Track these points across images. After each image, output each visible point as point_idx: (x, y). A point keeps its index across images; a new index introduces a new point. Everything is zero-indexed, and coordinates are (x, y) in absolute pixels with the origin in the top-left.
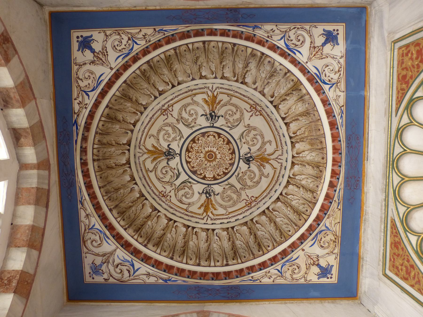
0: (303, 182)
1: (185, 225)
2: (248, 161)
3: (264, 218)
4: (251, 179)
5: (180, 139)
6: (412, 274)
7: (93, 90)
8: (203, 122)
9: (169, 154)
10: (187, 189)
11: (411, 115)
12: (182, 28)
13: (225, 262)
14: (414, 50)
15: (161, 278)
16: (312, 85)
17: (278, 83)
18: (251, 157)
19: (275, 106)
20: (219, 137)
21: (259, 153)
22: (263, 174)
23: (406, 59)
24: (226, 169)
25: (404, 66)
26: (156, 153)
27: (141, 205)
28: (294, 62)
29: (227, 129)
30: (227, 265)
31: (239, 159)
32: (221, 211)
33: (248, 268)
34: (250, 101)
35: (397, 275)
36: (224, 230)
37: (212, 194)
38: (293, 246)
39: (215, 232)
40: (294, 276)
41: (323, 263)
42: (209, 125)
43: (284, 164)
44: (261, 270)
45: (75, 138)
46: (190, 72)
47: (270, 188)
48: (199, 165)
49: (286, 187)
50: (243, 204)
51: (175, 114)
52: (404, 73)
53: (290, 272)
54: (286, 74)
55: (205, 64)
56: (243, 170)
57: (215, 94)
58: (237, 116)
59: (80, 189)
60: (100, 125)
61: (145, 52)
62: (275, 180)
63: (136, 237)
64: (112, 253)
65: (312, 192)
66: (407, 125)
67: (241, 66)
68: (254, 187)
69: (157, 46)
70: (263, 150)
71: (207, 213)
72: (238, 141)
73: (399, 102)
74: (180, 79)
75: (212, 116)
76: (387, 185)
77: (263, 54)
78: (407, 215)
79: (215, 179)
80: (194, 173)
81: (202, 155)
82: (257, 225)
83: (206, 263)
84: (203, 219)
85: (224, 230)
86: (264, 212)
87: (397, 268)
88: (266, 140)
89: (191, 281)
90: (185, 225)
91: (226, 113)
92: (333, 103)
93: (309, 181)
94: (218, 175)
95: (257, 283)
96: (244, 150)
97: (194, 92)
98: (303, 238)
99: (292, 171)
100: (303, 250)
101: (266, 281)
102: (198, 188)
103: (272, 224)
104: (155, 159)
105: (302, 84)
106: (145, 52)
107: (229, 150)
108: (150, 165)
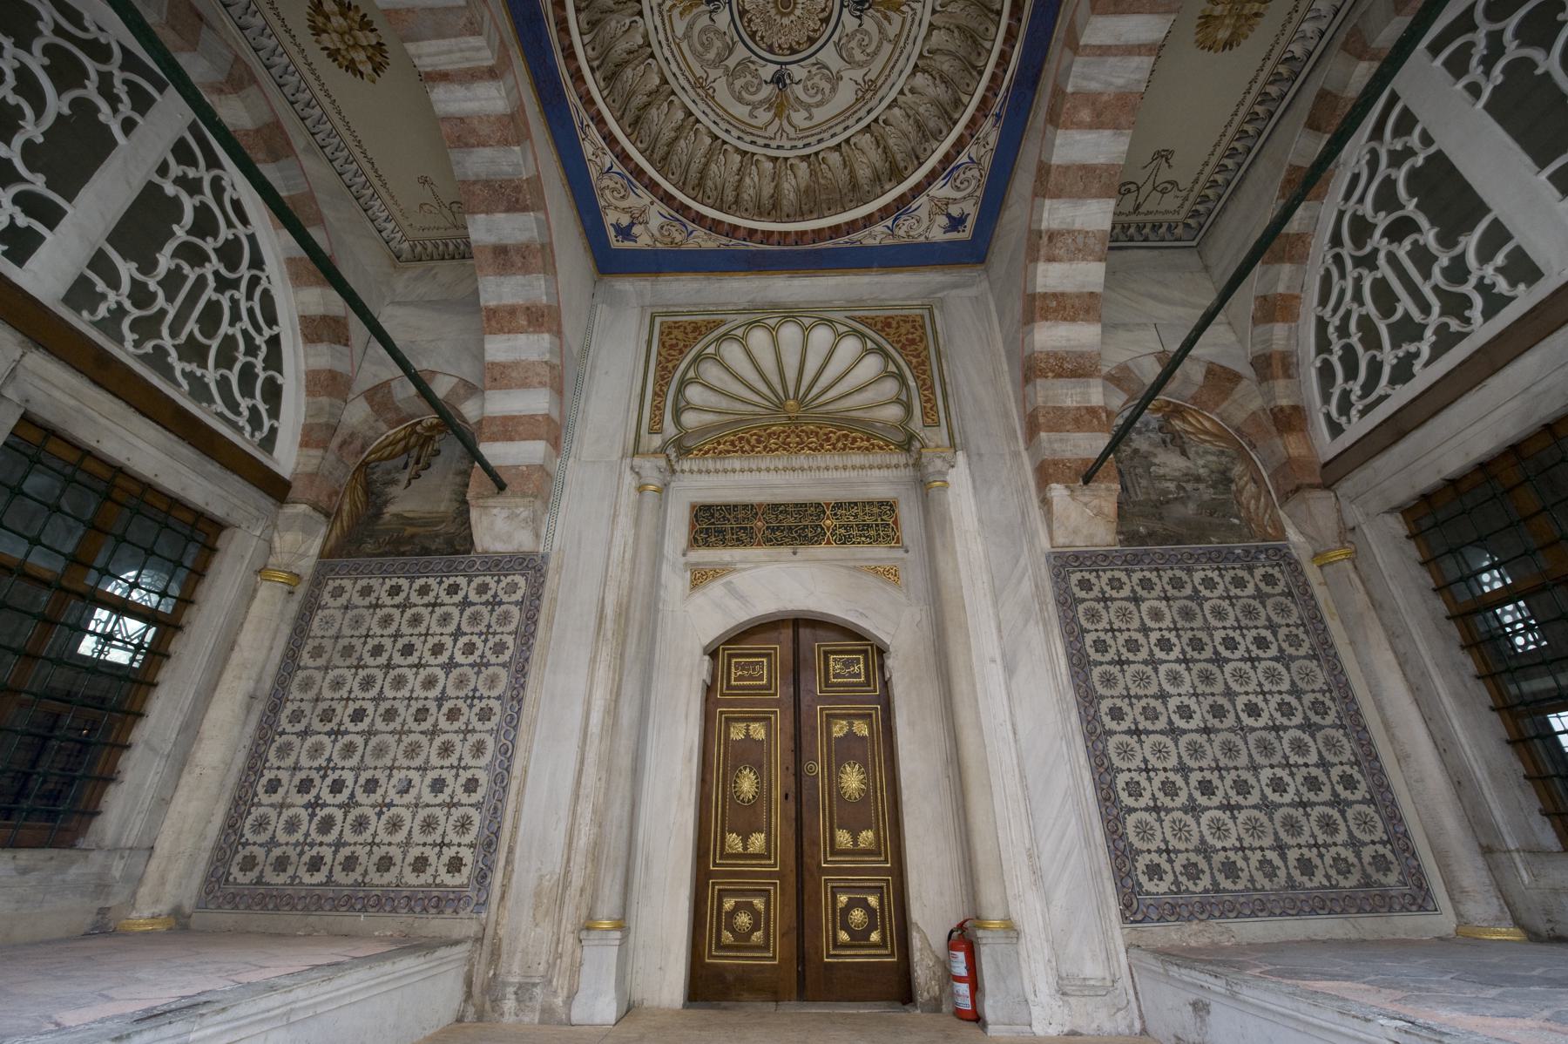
0: (747, 180)
2: (778, 79)
3: (680, 115)
4: (745, 87)
11: (846, 334)
13: (595, 64)
17: (905, 135)
18: (785, 85)
19: (869, 126)
20: (822, 21)
22: (755, 108)
23: (909, 326)
24: (762, 38)
28: (932, 177)
29: (835, 38)
30: (592, 70)
32: (680, 27)
33: (599, 112)
35: (662, 333)
36: (646, 36)
38: (652, 186)
39: (637, 18)
41: (636, 230)
43: (774, 144)
47: (733, 121)
49: (737, 150)
50: (699, 72)
52: (894, 324)
53: (612, 185)
56: (761, 71)
57: (904, 8)
58: (859, 57)
62: (745, 129)
66: (835, 331)
67: (945, 67)
68: (732, 92)
72: (813, 60)
73: (861, 320)
77: (955, 123)
78: (735, 339)
79: (743, 13)
83: (584, 26)
85: (646, 36)
88: (814, 110)
91: (867, 33)
93: (751, 191)
94: (750, 21)
95: (581, 135)
96: (797, 72)
98: (667, 199)
99: (763, 159)
101: (588, 149)
103: (673, 134)
107: (798, 43)
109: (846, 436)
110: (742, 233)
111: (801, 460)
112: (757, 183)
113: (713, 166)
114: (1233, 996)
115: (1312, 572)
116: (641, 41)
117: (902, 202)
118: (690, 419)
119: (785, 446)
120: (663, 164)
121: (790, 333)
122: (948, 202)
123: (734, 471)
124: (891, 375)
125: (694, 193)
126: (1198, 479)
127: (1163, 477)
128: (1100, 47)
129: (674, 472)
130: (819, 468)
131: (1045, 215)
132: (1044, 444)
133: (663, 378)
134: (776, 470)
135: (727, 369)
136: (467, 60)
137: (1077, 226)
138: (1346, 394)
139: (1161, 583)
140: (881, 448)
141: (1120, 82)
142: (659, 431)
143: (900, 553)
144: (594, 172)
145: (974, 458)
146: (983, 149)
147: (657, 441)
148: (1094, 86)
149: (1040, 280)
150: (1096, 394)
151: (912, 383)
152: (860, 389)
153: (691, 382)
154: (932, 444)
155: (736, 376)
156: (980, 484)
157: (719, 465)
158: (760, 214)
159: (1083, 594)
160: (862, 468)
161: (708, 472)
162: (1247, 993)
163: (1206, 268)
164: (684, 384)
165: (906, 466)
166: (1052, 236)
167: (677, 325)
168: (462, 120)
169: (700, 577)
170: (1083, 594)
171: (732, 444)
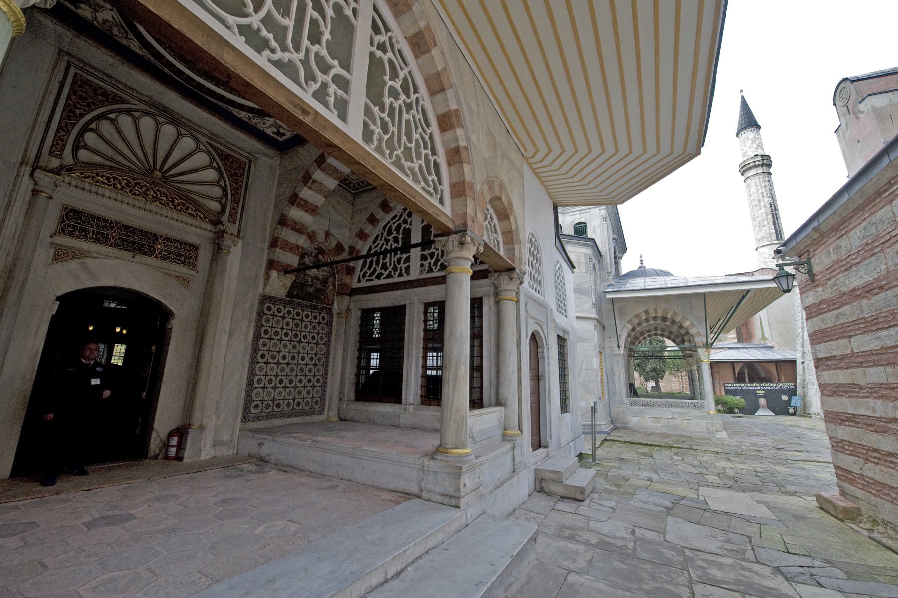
73: (216, 149)
111: (153, 207)
114: (274, 440)
115: (335, 317)
118: (84, 155)
119: (145, 195)
121: (168, 130)
126: (318, 279)
127: (309, 275)
135: (120, 132)
138: (366, 272)
139: (293, 313)
142: (60, 157)
143: (193, 272)
150: (302, 241)
151: (230, 197)
154: (229, 231)
155: (124, 140)
156: (245, 256)
157: (93, 188)
159: (267, 312)
162: (278, 439)
163: (353, 204)
164: (85, 129)
165: (210, 231)
166: (314, 181)
169: (60, 255)
170: (267, 312)
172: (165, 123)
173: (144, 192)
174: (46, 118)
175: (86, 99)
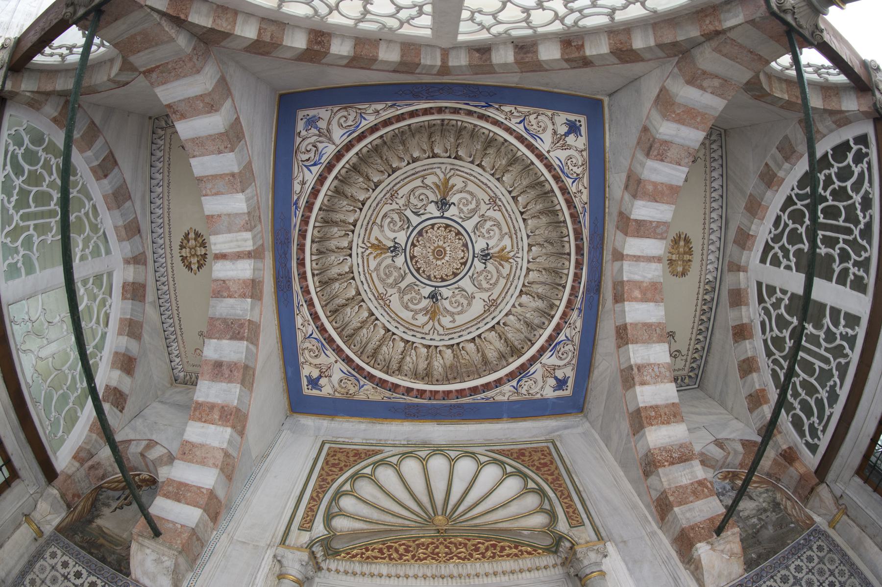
0: (408, 359)
1: (356, 221)
2: (433, 296)
3: (366, 314)
4: (411, 300)
5: (461, 218)
6: (334, 469)
7: (526, 129)
8: (480, 244)
9: (443, 204)
10: (399, 224)
12: (586, 233)
13: (316, 272)
14: (547, 460)
15: (298, 198)
16: (517, 368)
18: (437, 300)
19: (493, 327)
21: (441, 309)
23: (539, 454)
24: (424, 271)
25: (533, 453)
26: (445, 188)
27: (382, 169)
28: (542, 351)
29: (470, 274)
30: (313, 275)
31: (435, 287)
32: (373, 264)
33: (311, 299)
34: (501, 299)
35: (328, 454)
36: (351, 267)
37: (394, 254)
38: (339, 351)
40: (306, 351)
41: (323, 381)
42: (476, 252)
44: (311, 315)
45: (472, 103)
46: (537, 233)
47: (400, 321)
48: (429, 239)
49: (402, 339)
50: (381, 290)
51: (490, 213)
52: (527, 454)
53: (310, 347)
54: (530, 341)
55: (544, 251)
56: (422, 291)
57: (511, 260)
58: (485, 285)
59: (410, 105)
60: (484, 131)
61: (564, 190)
62: (409, 327)
63: (347, 166)
64: (331, 140)
65: (399, 369)
67: (540, 291)
68: (402, 303)
69: (570, 203)
70: (444, 313)
71: (371, 247)
72: (456, 286)
73: (499, 452)
74: (529, 222)
75: (486, 256)
76: (415, 445)
77: (553, 317)
80: (420, 233)
81: (441, 243)
82: (357, 307)
83: (314, 250)
84: (363, 242)
85: (351, 267)
86: (373, 314)
87: (335, 455)
88: (456, 317)
89: (295, 234)
90: (356, 221)
91: (489, 272)
92: (498, 390)
93: (410, 365)
94: (417, 262)
96: (445, 292)
97: (514, 236)
98: (348, 361)
99: (420, 346)
100: (336, 362)
101: (299, 321)
102: (401, 238)
103: (359, 325)
104: (437, 186)
105: (519, 357)
106: (564, 190)
107: (447, 275)
108: (430, 180)
109: (494, 546)
110: (401, 390)
111: (451, 568)
112: (417, 359)
113: (384, 348)
116: (347, 270)
117: (523, 369)
118: (340, 523)
119: (435, 556)
120: (349, 339)
121: (438, 464)
122: (555, 368)
123: (380, 576)
124: (532, 491)
125: (368, 360)
128: (635, 256)
129: (320, 569)
130: (469, 576)
131: (631, 355)
132: (680, 516)
133: (321, 487)
134: (425, 577)
136: (239, 247)
137: (652, 361)
140: (529, 553)
141: (650, 276)
142: (310, 529)
144: (300, 337)
145: (621, 544)
146: (573, 331)
147: (305, 537)
148: (637, 278)
149: (640, 398)
152: (504, 505)
153: (346, 493)
156: (633, 564)
157: (366, 568)
158: (416, 378)
160: (512, 572)
161: (354, 574)
164: (339, 494)
165: (554, 566)
167: (341, 451)
168: (224, 281)
171: (381, 551)
172: (430, 456)
173: (432, 553)
174: (298, 493)
175: (339, 464)
